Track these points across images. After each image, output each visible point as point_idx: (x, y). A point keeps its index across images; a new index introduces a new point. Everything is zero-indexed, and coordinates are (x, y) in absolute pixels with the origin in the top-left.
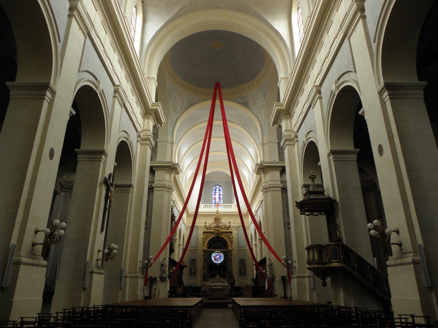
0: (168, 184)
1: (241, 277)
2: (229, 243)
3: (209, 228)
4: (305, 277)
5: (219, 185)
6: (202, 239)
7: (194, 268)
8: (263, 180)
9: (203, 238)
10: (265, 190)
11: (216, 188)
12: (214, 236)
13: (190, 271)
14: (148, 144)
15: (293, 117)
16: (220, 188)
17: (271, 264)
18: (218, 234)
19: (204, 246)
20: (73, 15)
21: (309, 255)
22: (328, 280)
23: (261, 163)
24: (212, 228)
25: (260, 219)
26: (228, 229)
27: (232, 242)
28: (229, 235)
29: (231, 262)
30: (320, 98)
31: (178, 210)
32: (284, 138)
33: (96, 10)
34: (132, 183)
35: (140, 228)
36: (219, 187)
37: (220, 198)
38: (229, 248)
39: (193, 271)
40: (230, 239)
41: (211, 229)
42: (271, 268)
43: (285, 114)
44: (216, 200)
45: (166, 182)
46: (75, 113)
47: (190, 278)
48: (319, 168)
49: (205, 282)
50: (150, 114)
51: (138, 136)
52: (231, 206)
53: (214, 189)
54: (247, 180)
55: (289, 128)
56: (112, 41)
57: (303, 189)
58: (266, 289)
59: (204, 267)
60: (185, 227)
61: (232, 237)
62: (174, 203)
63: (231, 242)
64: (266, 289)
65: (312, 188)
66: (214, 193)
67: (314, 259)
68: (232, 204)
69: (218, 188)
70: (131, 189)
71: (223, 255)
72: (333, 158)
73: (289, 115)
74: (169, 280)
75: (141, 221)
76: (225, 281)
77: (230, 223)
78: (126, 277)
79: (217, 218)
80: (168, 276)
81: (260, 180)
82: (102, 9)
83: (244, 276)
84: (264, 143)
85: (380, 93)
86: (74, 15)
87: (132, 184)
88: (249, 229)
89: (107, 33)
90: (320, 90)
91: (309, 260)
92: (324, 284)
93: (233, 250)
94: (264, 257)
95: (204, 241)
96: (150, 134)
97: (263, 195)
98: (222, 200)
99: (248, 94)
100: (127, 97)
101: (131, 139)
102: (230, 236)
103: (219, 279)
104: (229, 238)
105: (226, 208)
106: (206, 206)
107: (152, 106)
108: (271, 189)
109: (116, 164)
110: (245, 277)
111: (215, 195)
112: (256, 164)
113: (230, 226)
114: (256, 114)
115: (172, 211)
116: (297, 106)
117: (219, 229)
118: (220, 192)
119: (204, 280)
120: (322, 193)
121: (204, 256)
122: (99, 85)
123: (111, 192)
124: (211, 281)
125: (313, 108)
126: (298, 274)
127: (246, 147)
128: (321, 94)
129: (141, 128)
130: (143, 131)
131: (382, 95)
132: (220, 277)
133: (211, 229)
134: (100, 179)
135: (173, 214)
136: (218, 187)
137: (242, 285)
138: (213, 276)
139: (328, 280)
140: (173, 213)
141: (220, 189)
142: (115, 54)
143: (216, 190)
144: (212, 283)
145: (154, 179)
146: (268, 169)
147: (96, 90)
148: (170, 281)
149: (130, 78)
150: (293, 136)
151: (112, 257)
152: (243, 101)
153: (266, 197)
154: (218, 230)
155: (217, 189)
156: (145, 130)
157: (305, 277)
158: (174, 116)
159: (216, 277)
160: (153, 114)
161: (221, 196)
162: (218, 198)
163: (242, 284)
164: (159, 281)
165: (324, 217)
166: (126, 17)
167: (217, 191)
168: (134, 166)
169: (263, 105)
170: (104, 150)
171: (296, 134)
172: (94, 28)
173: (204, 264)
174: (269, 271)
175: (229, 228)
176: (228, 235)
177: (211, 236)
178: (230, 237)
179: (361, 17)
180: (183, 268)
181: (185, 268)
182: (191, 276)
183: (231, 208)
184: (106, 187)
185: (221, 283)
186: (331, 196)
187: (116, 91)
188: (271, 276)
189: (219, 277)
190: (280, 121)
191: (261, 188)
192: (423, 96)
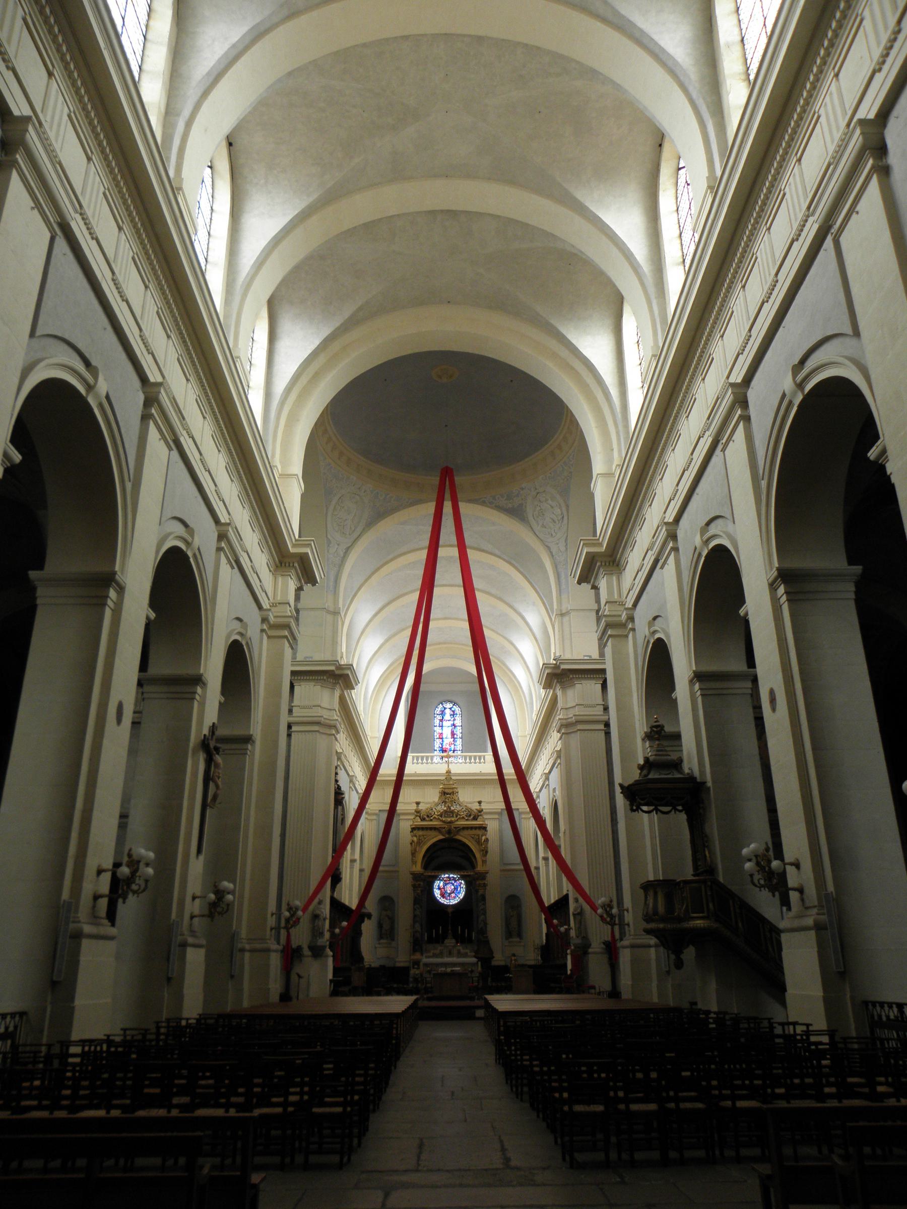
0: (326, 714)
2: (478, 855)
3: (428, 816)
4: (650, 946)
5: (451, 702)
6: (410, 845)
8: (560, 704)
9: (411, 844)
10: (566, 727)
11: (445, 708)
12: (441, 837)
13: (380, 926)
14: (286, 637)
15: (624, 569)
16: (457, 709)
17: (579, 910)
18: (449, 832)
20: (151, 416)
21: (647, 902)
22: (689, 954)
23: (555, 662)
24: (435, 818)
25: (554, 796)
26: (475, 818)
27: (485, 852)
28: (478, 835)
29: (484, 904)
30: (676, 549)
31: (348, 774)
32: (604, 620)
33: (188, 380)
34: (251, 733)
35: (270, 834)
36: (451, 705)
37: (455, 736)
38: (480, 868)
40: (482, 845)
42: (580, 923)
43: (605, 564)
44: (444, 740)
45: (320, 712)
46: (154, 615)
47: (379, 944)
48: (674, 702)
49: (417, 956)
50: (289, 566)
51: (264, 620)
52: (484, 759)
53: (438, 711)
54: (523, 691)
55: (616, 597)
56: (181, 355)
57: (646, 742)
58: (569, 972)
59: (415, 916)
61: (487, 840)
62: (339, 759)
64: (569, 972)
65: (656, 755)
66: (438, 721)
67: (655, 912)
68: (486, 752)
69: (450, 709)
70: (249, 747)
72: (700, 689)
73: (615, 565)
74: (331, 953)
75: (273, 820)
76: (468, 951)
77: (480, 802)
78: (242, 950)
79: (446, 791)
80: (328, 943)
81: (554, 702)
82: (160, 284)
83: (518, 939)
84: (564, 612)
85: (773, 586)
86: (152, 415)
87: (252, 735)
89: (190, 380)
90: (676, 533)
91: (647, 913)
92: (679, 964)
93: (488, 873)
94: (565, 892)
95: (415, 850)
96: (290, 614)
97: (560, 739)
98: (459, 742)
99: (522, 489)
100: (241, 540)
101: (249, 633)
102: (482, 836)
104: (478, 842)
105: (470, 763)
106: (417, 760)
107: (294, 546)
108: (580, 727)
109: (223, 699)
110: (520, 942)
111: (442, 726)
112: (543, 664)
113: (480, 811)
114: (542, 538)
115: (336, 781)
116: (632, 550)
117: (453, 819)
118: (454, 720)
119: (414, 950)
120: (677, 765)
121: (414, 888)
122: (193, 539)
123: (217, 766)
124: (432, 951)
125: (662, 568)
126: (633, 939)
127: (521, 610)
128: (677, 540)
129: (269, 600)
130: (274, 605)
131: (776, 590)
132: (457, 943)
133: (431, 820)
134: (194, 739)
135: (339, 788)
136: (449, 705)
137: (513, 962)
138: (439, 940)
139: (689, 954)
140: (338, 785)
141: (453, 711)
142: (206, 422)
143: (443, 713)
144: (437, 957)
145: (293, 705)
146: (571, 676)
147: (187, 550)
148: (333, 956)
149: (248, 496)
150: (624, 617)
151: (223, 910)
152: (510, 506)
153: (566, 746)
154: (451, 822)
155: (448, 712)
156: (279, 603)
157: (650, 946)
158: (338, 545)
159: (446, 941)
160: (296, 565)
161: (458, 731)
162: (450, 736)
163: (513, 958)
164: (308, 956)
165: (683, 817)
166: (238, 357)
167: (447, 716)
168: (255, 693)
169: (560, 517)
170: (201, 675)
171: (630, 612)
172: (184, 422)
173: (415, 910)
174: (575, 929)
175: (479, 816)
177: (433, 838)
178: (481, 840)
179: (741, 417)
180: (363, 921)
181: (366, 919)
182: (382, 941)
183: (484, 763)
184: (205, 755)
186: (697, 773)
187: (222, 537)
188: (578, 941)
189: (454, 941)
190: (596, 578)
191: (555, 724)
192: (853, 596)
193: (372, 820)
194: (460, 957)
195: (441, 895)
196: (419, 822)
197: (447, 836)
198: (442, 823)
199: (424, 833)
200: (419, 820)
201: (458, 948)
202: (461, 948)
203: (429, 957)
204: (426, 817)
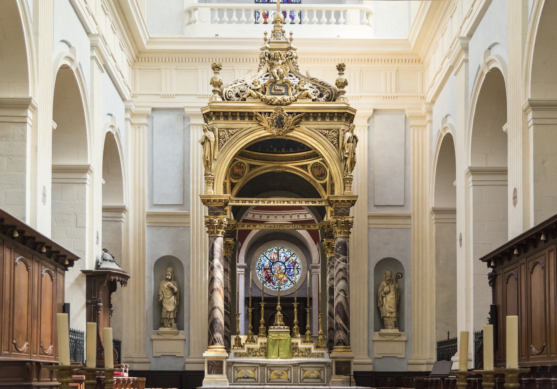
3: (237, 95)
6: (200, 146)
9: (203, 144)
12: (263, 133)
19: (209, 180)
24: (250, 95)
39: (170, 305)
40: (343, 148)
41: (248, 100)
63: (348, 162)
76: (312, 346)
117: (286, 97)
154: (280, 104)
159: (272, 329)
176: (329, 130)
189: (286, 329)
196: (219, 103)
197: (275, 131)
198: (262, 105)
200: (221, 100)
204: (234, 96)
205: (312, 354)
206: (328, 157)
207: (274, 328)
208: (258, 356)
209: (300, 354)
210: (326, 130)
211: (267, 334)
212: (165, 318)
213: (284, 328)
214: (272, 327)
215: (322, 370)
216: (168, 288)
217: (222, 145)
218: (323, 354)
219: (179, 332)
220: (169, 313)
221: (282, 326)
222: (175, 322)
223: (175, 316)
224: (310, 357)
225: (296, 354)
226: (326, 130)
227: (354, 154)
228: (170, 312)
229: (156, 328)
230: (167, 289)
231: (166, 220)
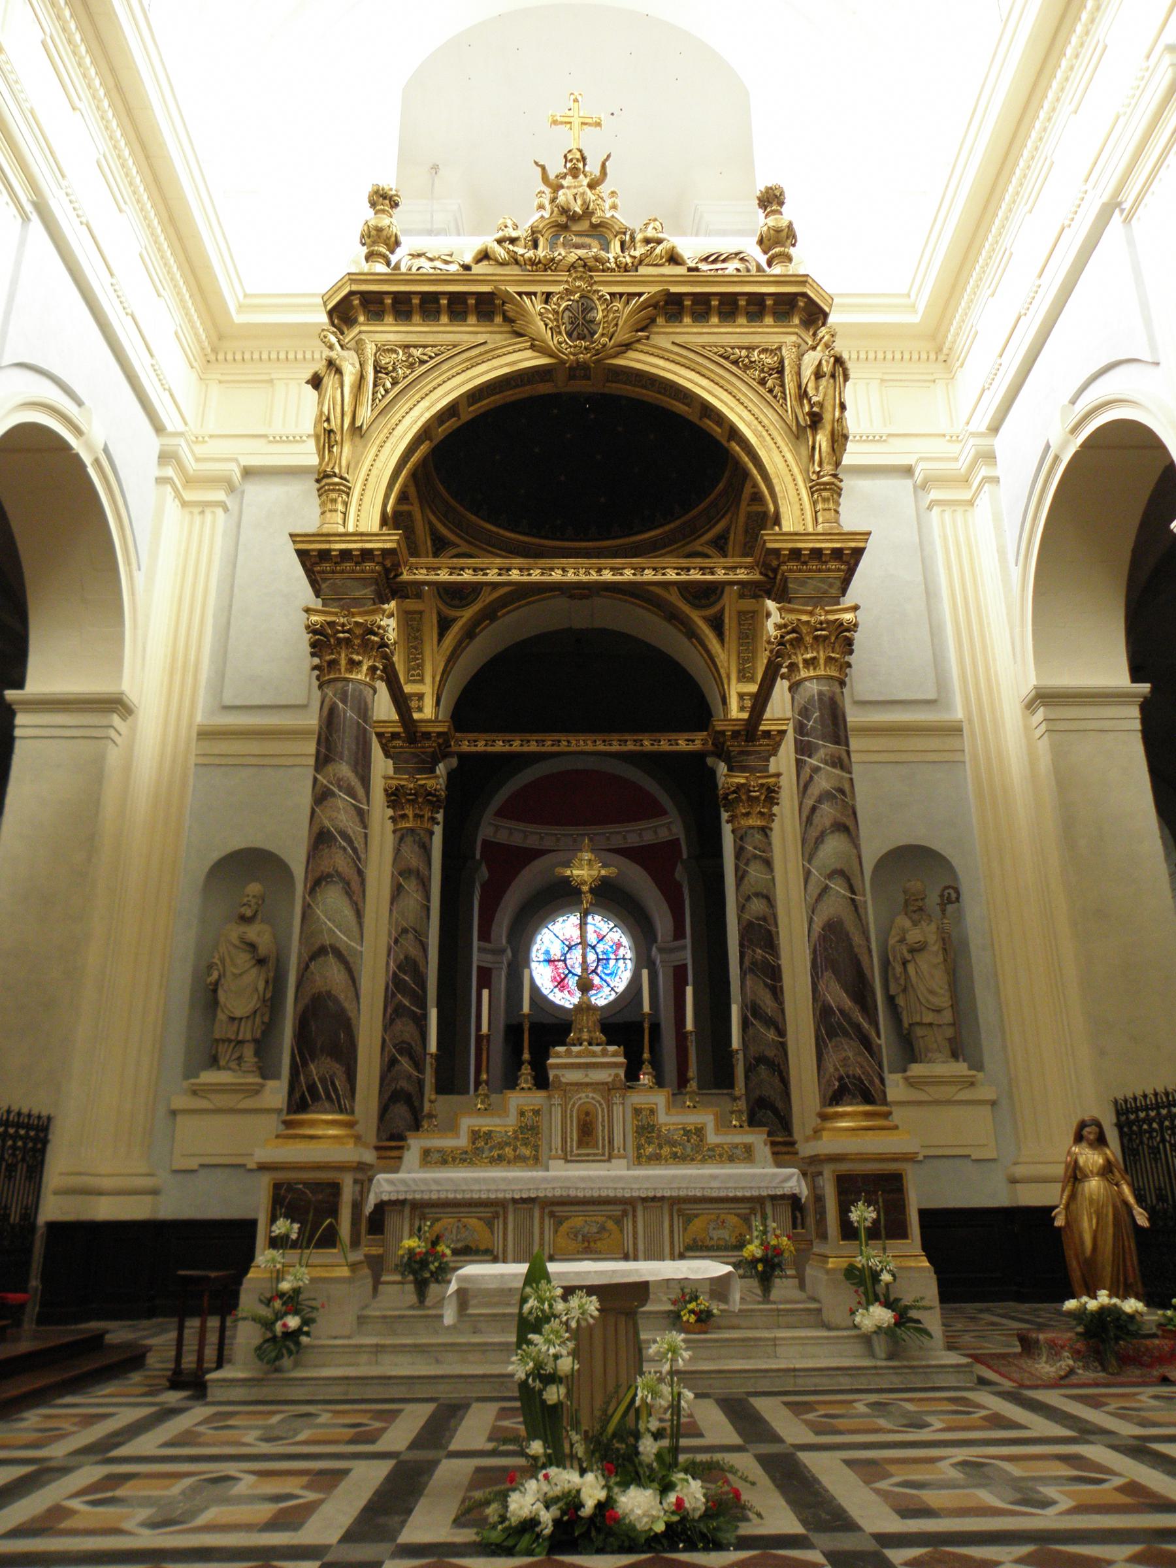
1: (911, 1083)
7: (261, 962)
12: (529, 360)
29: (841, 763)
60: (165, 457)
71: (625, 941)
76: (705, 1118)
77: (771, 200)
83: (961, 1068)
88: (971, 503)
103: (607, 1089)
124: (467, 1123)
132: (632, 1074)
144: (499, 1160)
173: (321, 797)
182: (209, 1077)
185: (640, 1159)
193: (204, 505)
194: (655, 1159)
195: (554, 979)
199: (417, 331)
201: (637, 1099)
202: (659, 1099)
203: (446, 1159)
205: (709, 1150)
206: (749, 425)
207: (569, 1054)
208: (509, 1162)
209: (666, 1151)
210: (741, 348)
211: (542, 1082)
212: (223, 1041)
213: (604, 1053)
214: (561, 1049)
215: (753, 1211)
216: (241, 945)
217: (387, 391)
218: (748, 1149)
219: (262, 1086)
220: (236, 1022)
221: (598, 1045)
222: (257, 1053)
223: (258, 1035)
224: (703, 1161)
225: (650, 1150)
226: (741, 348)
227: (843, 407)
228: (241, 1019)
229: (190, 1072)
230: (235, 946)
231: (253, 747)
